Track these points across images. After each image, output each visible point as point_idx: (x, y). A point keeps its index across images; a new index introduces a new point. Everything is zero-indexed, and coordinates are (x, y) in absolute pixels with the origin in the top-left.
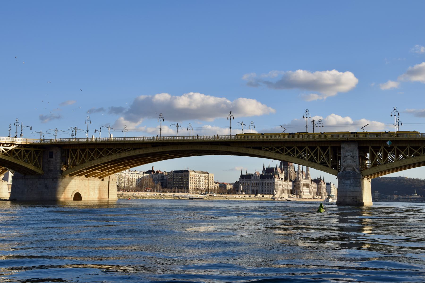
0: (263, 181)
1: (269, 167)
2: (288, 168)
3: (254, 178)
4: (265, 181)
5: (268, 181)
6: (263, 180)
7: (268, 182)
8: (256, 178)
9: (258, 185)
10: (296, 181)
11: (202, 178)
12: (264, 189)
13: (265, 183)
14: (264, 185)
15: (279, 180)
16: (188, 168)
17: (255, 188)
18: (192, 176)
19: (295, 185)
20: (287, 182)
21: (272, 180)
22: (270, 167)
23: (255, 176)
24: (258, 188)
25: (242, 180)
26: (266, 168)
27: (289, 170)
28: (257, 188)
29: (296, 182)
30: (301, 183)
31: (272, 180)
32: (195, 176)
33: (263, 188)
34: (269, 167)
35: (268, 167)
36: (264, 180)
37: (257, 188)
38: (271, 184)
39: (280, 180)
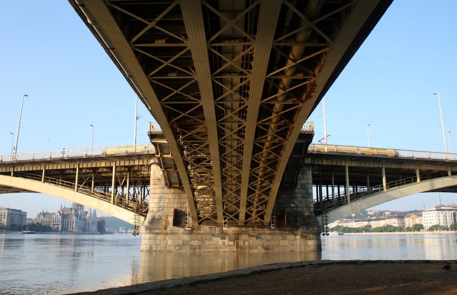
1: (65, 207)
8: (58, 217)
11: (17, 215)
22: (66, 207)
23: (57, 215)
26: (63, 208)
29: (87, 221)
32: (12, 214)
34: (65, 207)
35: (64, 207)
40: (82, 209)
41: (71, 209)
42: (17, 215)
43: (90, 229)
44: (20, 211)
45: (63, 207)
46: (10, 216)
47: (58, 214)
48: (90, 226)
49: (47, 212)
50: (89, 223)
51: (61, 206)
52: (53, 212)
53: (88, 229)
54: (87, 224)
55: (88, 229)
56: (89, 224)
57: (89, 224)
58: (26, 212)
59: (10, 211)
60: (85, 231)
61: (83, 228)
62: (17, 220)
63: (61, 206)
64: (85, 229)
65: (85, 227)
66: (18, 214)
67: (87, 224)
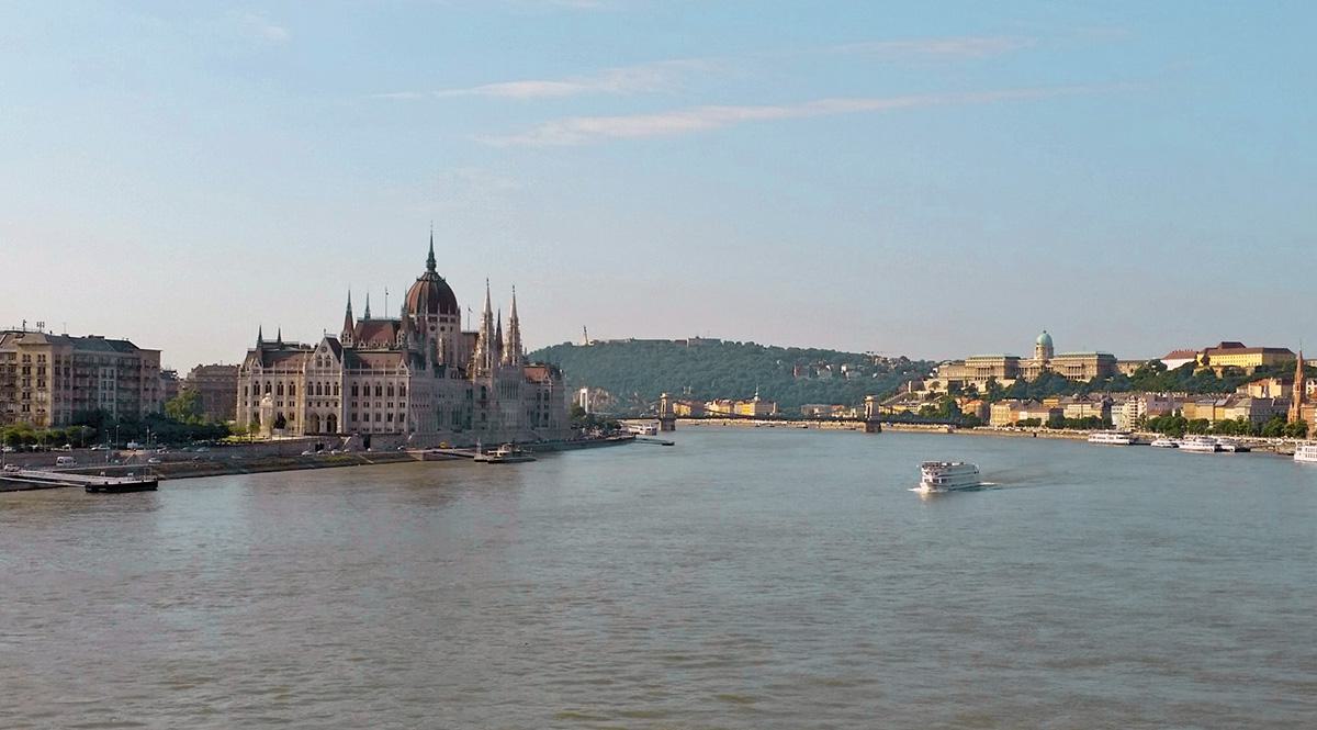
0: (355, 379)
1: (367, 316)
3: (320, 364)
4: (365, 379)
9: (336, 393)
11: (108, 369)
12: (361, 410)
14: (361, 392)
16: (40, 325)
17: (323, 405)
18: (63, 363)
24: (336, 405)
25: (261, 373)
28: (332, 405)
33: (355, 405)
34: (367, 316)
37: (332, 405)
41: (396, 325)
42: (107, 365)
44: (125, 346)
45: (358, 315)
46: (71, 372)
47: (332, 355)
48: (492, 404)
51: (349, 314)
53: (484, 416)
55: (484, 416)
56: (484, 396)
57: (484, 396)
58: (159, 352)
59: (67, 351)
62: (107, 392)
63: (349, 314)
66: (113, 361)
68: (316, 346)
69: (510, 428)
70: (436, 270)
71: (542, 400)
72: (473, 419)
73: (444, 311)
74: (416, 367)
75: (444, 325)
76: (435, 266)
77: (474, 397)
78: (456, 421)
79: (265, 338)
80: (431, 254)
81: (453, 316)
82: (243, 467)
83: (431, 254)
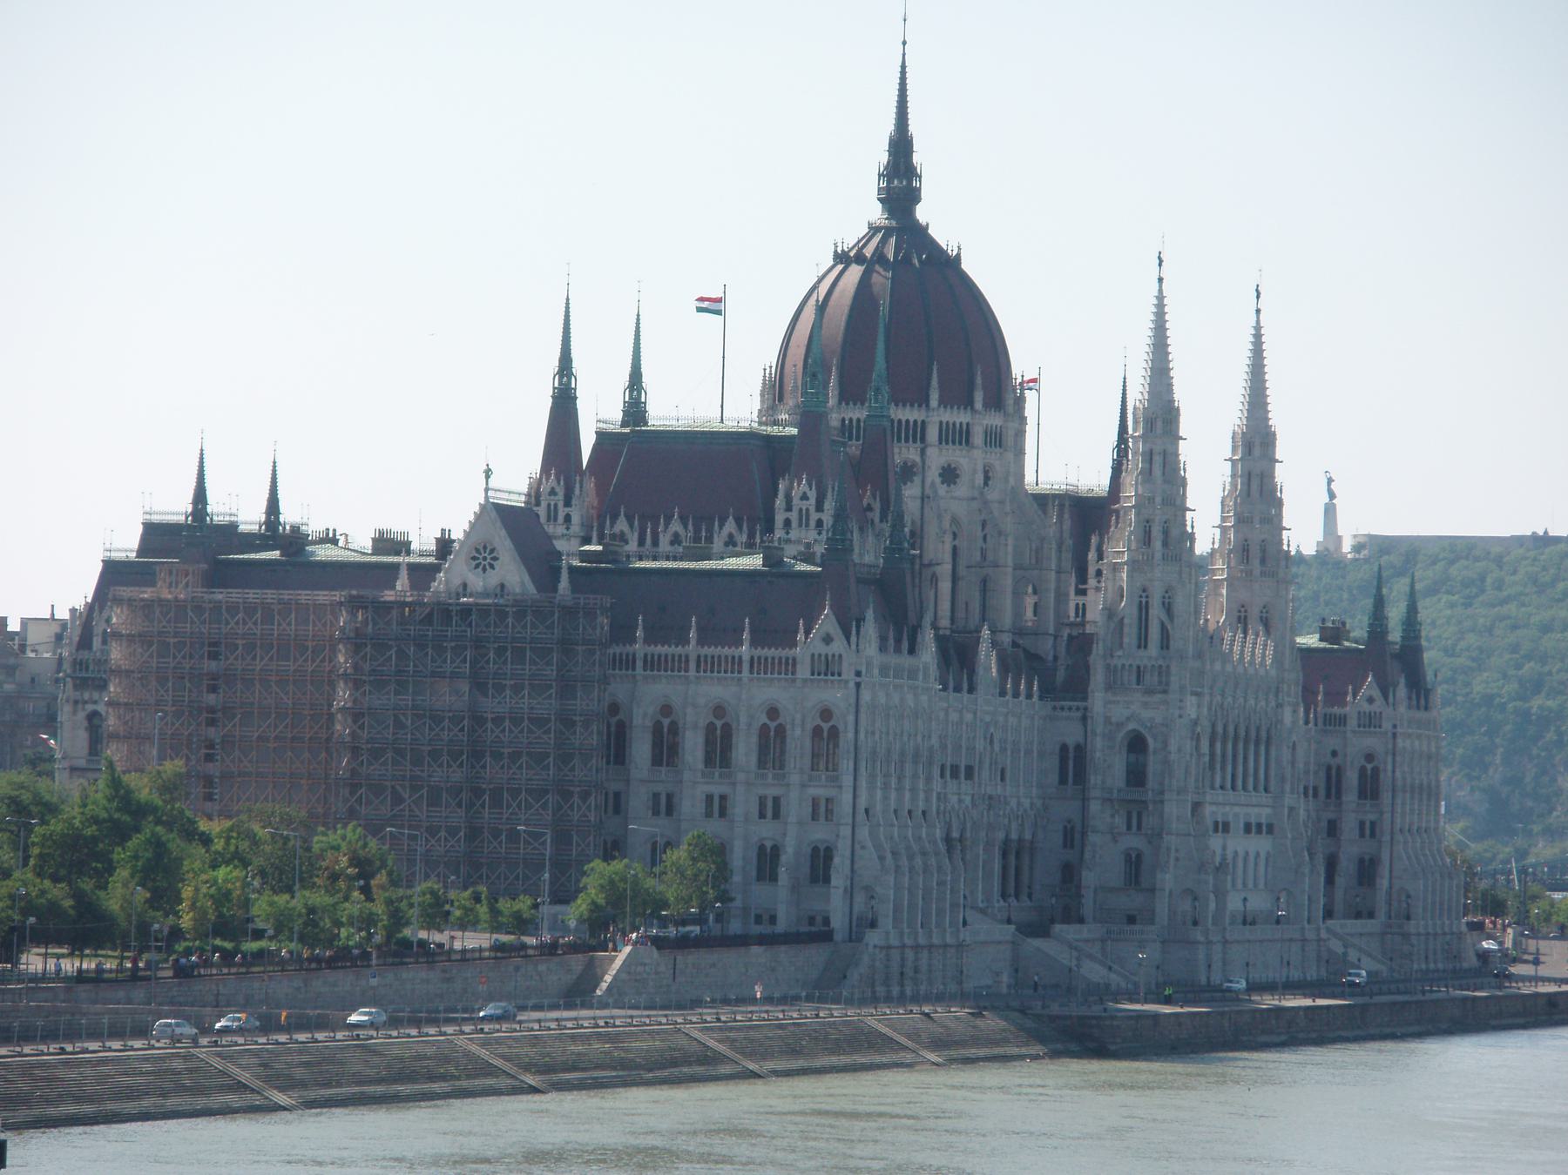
1: (635, 410)
2: (932, 434)
5: (712, 690)
6: (630, 662)
7: (719, 710)
10: (1098, 678)
13: (666, 710)
15: (906, 661)
19: (1080, 750)
20: (971, 690)
21: (803, 672)
22: (664, 412)
26: (602, 436)
27: (950, 475)
29: (1098, 699)
30: (1191, 708)
31: (790, 665)
34: (635, 410)
35: (613, 413)
36: (651, 663)
38: (772, 743)
39: (912, 674)
40: (995, 439)
43: (1167, 880)
48: (1175, 810)
49: (289, 515)
50: (1137, 744)
52: (396, 525)
53: (1135, 869)
54: (1110, 768)
56: (1136, 777)
57: (1136, 777)
60: (1072, 915)
61: (1015, 854)
64: (1069, 874)
65: (1073, 836)
67: (1110, 768)
68: (445, 545)
69: (1248, 921)
70: (922, 213)
71: (1350, 797)
72: (1089, 878)
73: (960, 397)
74: (883, 648)
75: (955, 455)
76: (913, 196)
77: (1094, 779)
78: (1013, 883)
79: (219, 507)
80: (901, 146)
81: (994, 420)
82: (527, 1068)
83: (901, 146)
